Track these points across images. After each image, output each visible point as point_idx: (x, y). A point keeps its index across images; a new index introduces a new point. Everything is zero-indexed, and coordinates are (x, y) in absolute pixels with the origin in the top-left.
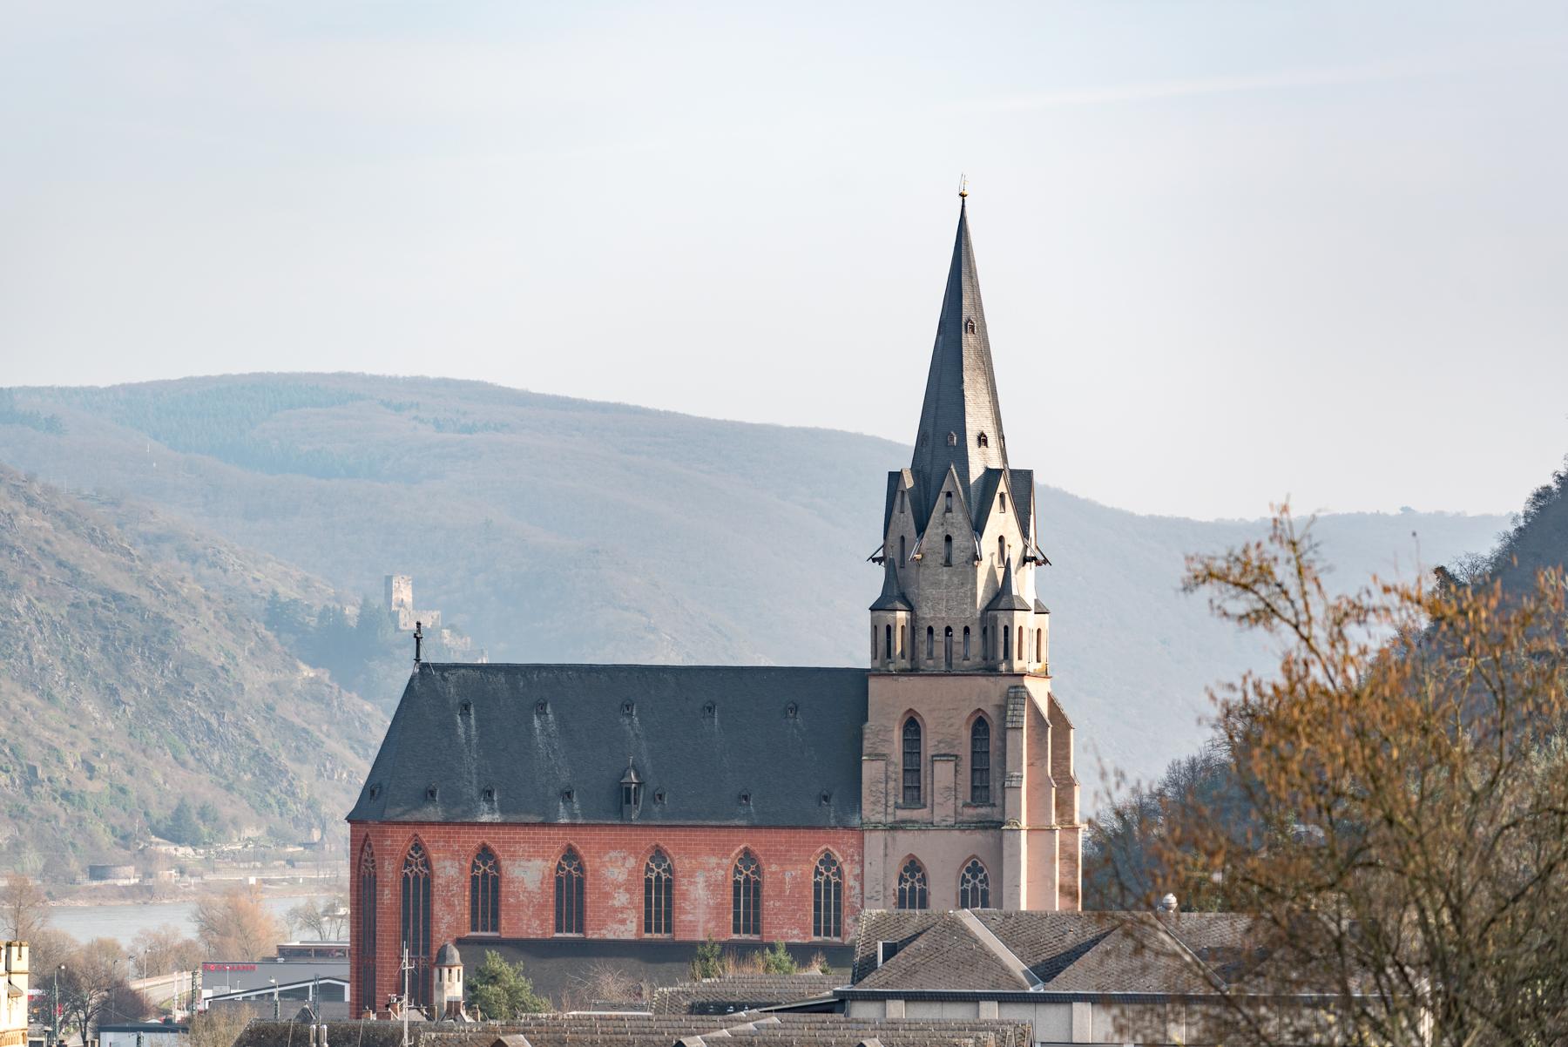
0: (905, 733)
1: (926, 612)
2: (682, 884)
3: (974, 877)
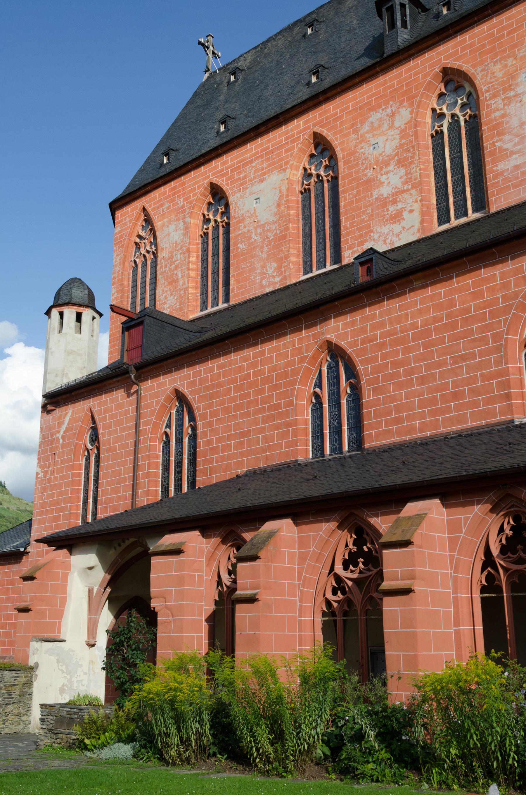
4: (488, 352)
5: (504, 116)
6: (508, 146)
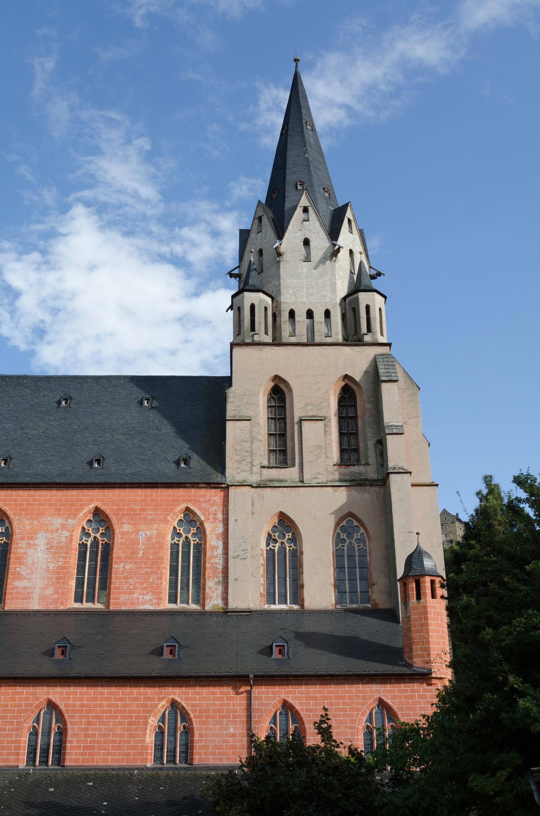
0: (269, 400)
1: (289, 299)
2: (19, 547)
3: (350, 536)
4: (13, 730)
5: (25, 553)
6: (23, 573)
